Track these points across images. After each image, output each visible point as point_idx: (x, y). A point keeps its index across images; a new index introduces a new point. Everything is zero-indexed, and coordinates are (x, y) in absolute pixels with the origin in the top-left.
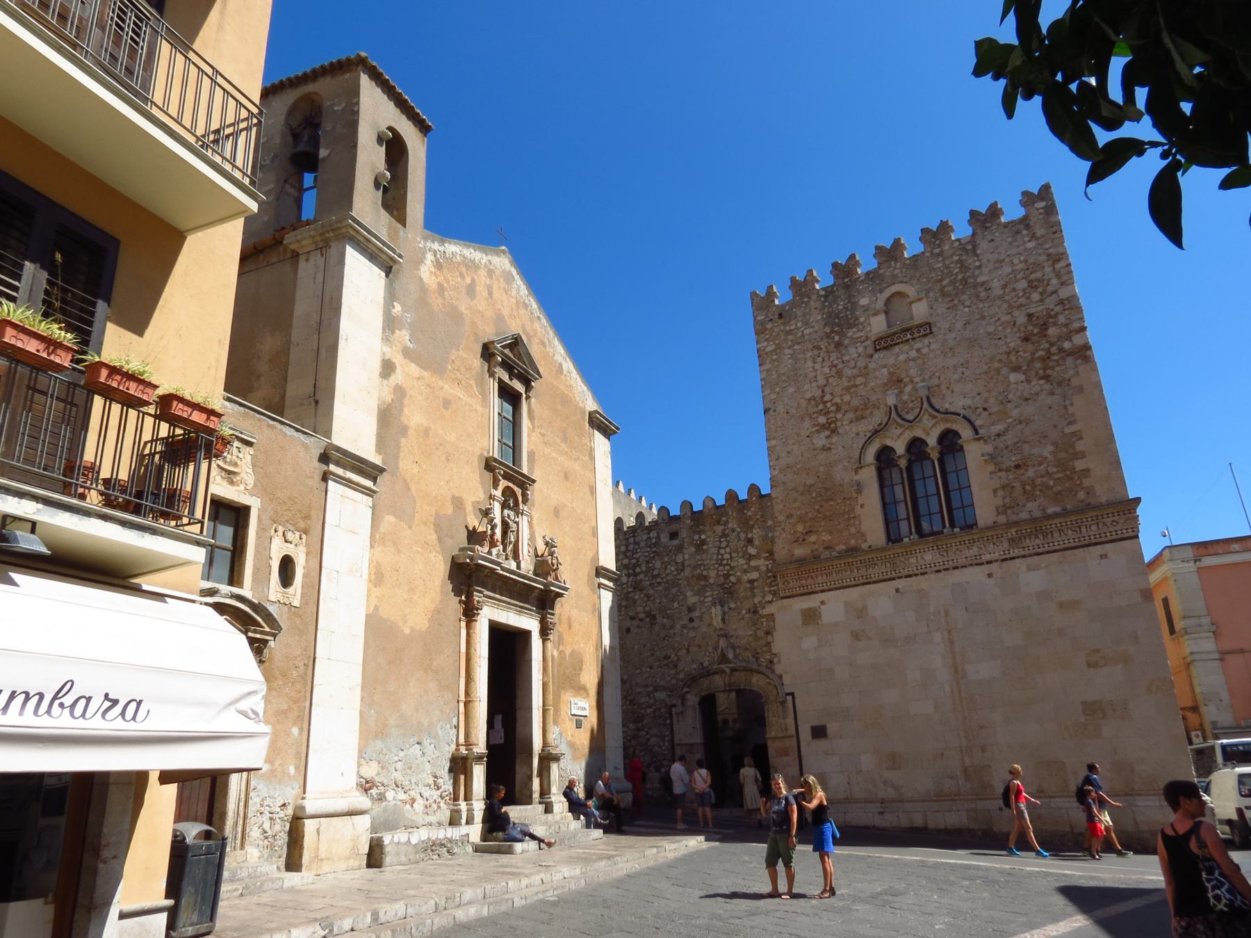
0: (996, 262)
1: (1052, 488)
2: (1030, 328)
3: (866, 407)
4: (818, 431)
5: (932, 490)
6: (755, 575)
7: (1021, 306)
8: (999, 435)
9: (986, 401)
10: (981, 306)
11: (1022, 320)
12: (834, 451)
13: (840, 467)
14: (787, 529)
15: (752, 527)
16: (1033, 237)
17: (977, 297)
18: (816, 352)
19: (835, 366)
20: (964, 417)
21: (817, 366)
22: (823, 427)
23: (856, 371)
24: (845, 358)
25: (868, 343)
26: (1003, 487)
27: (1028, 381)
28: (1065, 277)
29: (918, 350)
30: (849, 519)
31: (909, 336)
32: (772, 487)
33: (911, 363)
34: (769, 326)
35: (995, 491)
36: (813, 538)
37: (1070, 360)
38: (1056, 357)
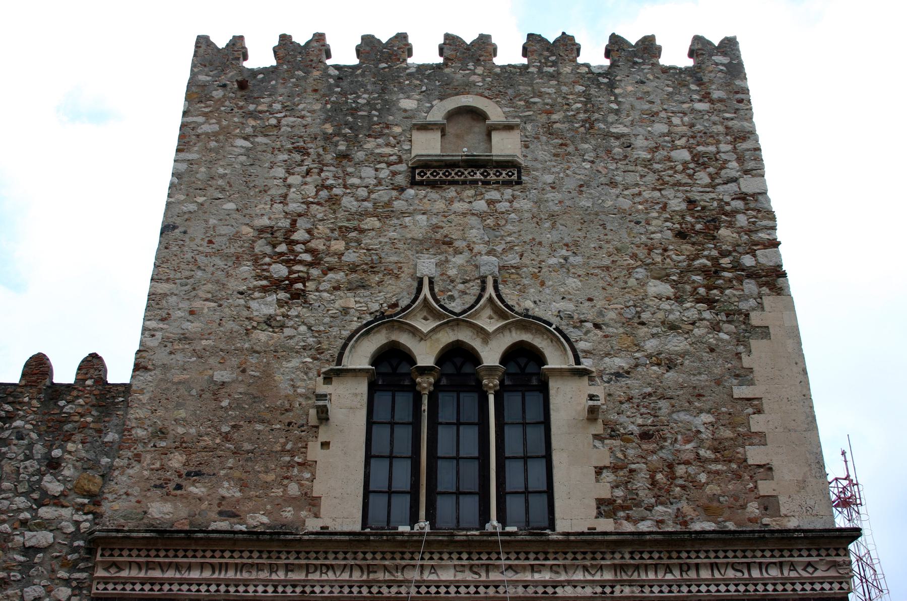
0: (643, 112)
1: (700, 486)
2: (689, 219)
3: (372, 268)
4: (264, 289)
5: (470, 447)
6: (44, 538)
7: (678, 184)
8: (618, 375)
9: (601, 314)
10: (613, 166)
11: (677, 204)
12: (288, 332)
13: (295, 362)
14: (147, 458)
15: (68, 438)
16: (706, 97)
17: (609, 151)
18: (298, 157)
19: (330, 188)
20: (557, 329)
21: (294, 180)
22: (276, 285)
23: (368, 205)
24: (355, 181)
25: (402, 167)
26: (615, 468)
27: (679, 299)
28: (752, 162)
29: (490, 202)
30: (290, 466)
31: (478, 176)
32: (137, 367)
33: (474, 221)
34: (218, 94)
35: (599, 471)
36: (197, 490)
37: (750, 286)
38: (726, 274)
